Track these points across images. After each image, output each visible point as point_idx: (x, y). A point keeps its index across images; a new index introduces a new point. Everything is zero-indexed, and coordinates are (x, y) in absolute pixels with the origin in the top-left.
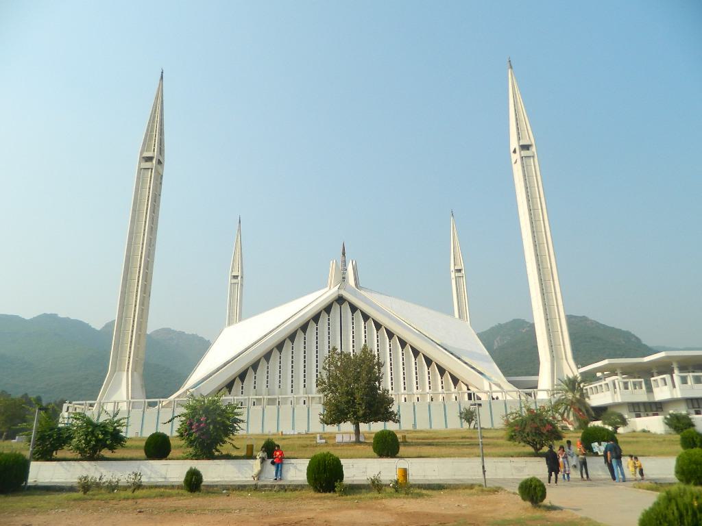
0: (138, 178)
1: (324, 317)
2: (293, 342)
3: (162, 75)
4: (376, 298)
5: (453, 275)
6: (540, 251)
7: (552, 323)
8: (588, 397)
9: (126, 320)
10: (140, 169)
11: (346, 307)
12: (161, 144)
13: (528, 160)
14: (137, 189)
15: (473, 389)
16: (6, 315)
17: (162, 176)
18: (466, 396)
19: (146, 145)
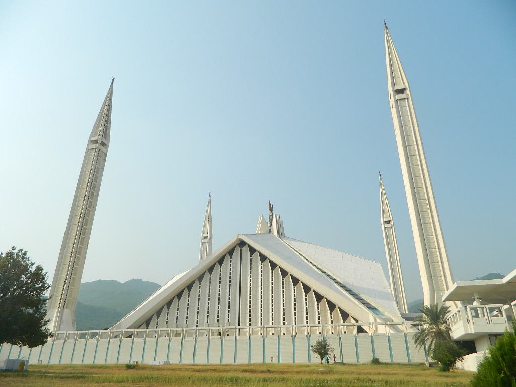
0: (85, 156)
1: (228, 258)
4: (295, 245)
5: (383, 228)
6: (416, 183)
7: (431, 253)
8: (451, 329)
9: (63, 268)
10: (88, 150)
11: (246, 250)
12: (106, 130)
13: (402, 102)
15: (360, 323)
16: (109, 280)
17: (106, 154)
18: (356, 331)
19: (93, 133)
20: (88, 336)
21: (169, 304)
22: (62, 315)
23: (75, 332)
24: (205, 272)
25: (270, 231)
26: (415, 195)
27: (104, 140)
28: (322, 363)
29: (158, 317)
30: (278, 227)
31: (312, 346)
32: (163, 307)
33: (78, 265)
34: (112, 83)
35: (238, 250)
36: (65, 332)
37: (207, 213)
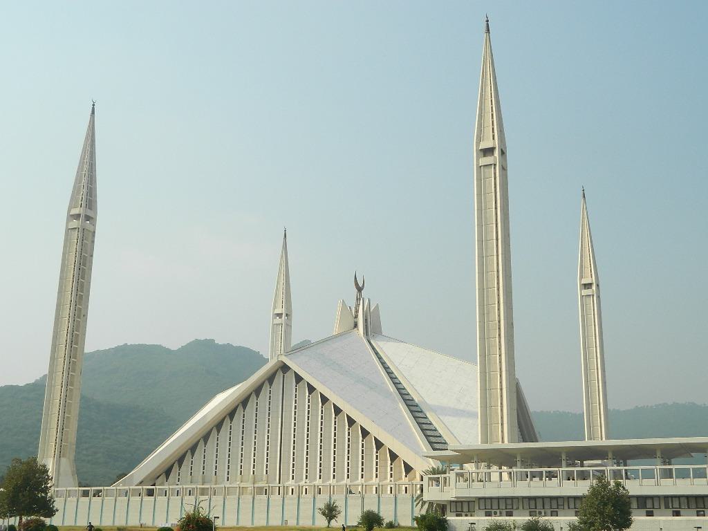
0: (66, 240)
2: (231, 420)
3: (93, 109)
14: (64, 254)
17: (94, 232)
20: (91, 494)
21: (193, 449)
22: (59, 466)
23: (77, 488)
24: (237, 407)
25: (356, 325)
26: (484, 314)
27: (90, 213)
28: (328, 527)
29: (180, 467)
30: (366, 321)
31: (320, 509)
32: (187, 451)
33: (71, 399)
34: (93, 112)
35: (280, 375)
36: (65, 489)
37: (281, 265)
